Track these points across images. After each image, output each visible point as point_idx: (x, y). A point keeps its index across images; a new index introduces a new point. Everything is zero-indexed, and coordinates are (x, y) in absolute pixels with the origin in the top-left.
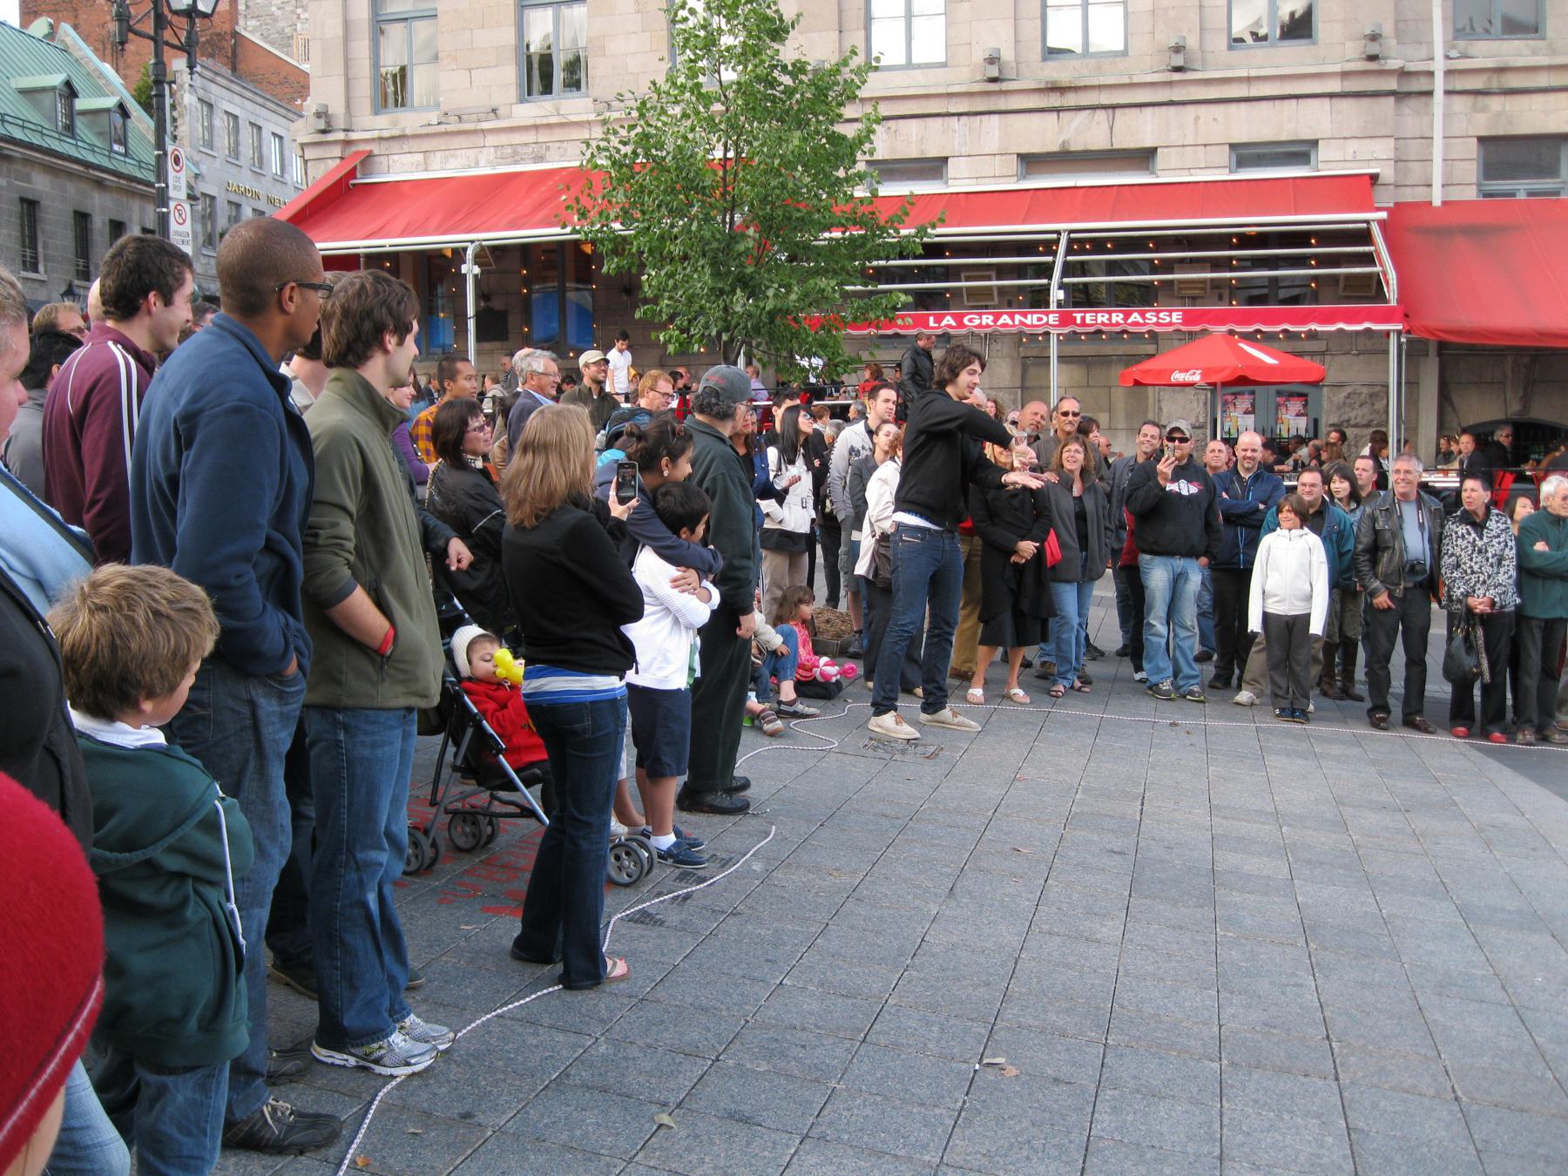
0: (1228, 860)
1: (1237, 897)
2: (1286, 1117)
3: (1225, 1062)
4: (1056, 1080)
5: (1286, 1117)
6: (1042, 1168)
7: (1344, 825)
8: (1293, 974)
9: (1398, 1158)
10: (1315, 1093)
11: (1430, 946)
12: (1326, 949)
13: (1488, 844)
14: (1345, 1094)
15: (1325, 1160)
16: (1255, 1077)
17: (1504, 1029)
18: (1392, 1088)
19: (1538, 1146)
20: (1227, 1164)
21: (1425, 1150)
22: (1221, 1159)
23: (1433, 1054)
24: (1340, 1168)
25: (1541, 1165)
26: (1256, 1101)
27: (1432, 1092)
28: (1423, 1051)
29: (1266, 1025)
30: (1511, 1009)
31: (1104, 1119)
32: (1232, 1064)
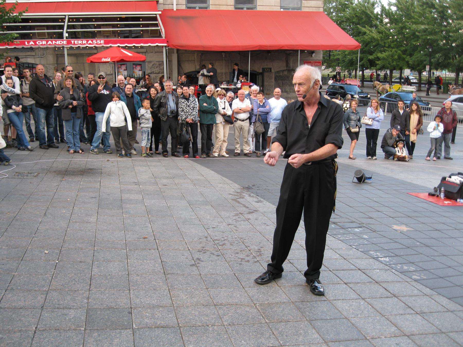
0: (126, 196)
1: (128, 206)
2: (145, 261)
3: (128, 250)
4: (81, 262)
5: (145, 261)
6: (79, 286)
7: (157, 184)
8: (145, 224)
11: (181, 212)
12: (153, 216)
13: (195, 185)
15: (156, 270)
16: (136, 252)
17: (200, 231)
18: (172, 250)
20: (130, 276)
22: (128, 275)
23: (182, 239)
26: (137, 258)
27: (183, 249)
28: (180, 239)
29: (138, 238)
31: (95, 270)
32: (130, 250)
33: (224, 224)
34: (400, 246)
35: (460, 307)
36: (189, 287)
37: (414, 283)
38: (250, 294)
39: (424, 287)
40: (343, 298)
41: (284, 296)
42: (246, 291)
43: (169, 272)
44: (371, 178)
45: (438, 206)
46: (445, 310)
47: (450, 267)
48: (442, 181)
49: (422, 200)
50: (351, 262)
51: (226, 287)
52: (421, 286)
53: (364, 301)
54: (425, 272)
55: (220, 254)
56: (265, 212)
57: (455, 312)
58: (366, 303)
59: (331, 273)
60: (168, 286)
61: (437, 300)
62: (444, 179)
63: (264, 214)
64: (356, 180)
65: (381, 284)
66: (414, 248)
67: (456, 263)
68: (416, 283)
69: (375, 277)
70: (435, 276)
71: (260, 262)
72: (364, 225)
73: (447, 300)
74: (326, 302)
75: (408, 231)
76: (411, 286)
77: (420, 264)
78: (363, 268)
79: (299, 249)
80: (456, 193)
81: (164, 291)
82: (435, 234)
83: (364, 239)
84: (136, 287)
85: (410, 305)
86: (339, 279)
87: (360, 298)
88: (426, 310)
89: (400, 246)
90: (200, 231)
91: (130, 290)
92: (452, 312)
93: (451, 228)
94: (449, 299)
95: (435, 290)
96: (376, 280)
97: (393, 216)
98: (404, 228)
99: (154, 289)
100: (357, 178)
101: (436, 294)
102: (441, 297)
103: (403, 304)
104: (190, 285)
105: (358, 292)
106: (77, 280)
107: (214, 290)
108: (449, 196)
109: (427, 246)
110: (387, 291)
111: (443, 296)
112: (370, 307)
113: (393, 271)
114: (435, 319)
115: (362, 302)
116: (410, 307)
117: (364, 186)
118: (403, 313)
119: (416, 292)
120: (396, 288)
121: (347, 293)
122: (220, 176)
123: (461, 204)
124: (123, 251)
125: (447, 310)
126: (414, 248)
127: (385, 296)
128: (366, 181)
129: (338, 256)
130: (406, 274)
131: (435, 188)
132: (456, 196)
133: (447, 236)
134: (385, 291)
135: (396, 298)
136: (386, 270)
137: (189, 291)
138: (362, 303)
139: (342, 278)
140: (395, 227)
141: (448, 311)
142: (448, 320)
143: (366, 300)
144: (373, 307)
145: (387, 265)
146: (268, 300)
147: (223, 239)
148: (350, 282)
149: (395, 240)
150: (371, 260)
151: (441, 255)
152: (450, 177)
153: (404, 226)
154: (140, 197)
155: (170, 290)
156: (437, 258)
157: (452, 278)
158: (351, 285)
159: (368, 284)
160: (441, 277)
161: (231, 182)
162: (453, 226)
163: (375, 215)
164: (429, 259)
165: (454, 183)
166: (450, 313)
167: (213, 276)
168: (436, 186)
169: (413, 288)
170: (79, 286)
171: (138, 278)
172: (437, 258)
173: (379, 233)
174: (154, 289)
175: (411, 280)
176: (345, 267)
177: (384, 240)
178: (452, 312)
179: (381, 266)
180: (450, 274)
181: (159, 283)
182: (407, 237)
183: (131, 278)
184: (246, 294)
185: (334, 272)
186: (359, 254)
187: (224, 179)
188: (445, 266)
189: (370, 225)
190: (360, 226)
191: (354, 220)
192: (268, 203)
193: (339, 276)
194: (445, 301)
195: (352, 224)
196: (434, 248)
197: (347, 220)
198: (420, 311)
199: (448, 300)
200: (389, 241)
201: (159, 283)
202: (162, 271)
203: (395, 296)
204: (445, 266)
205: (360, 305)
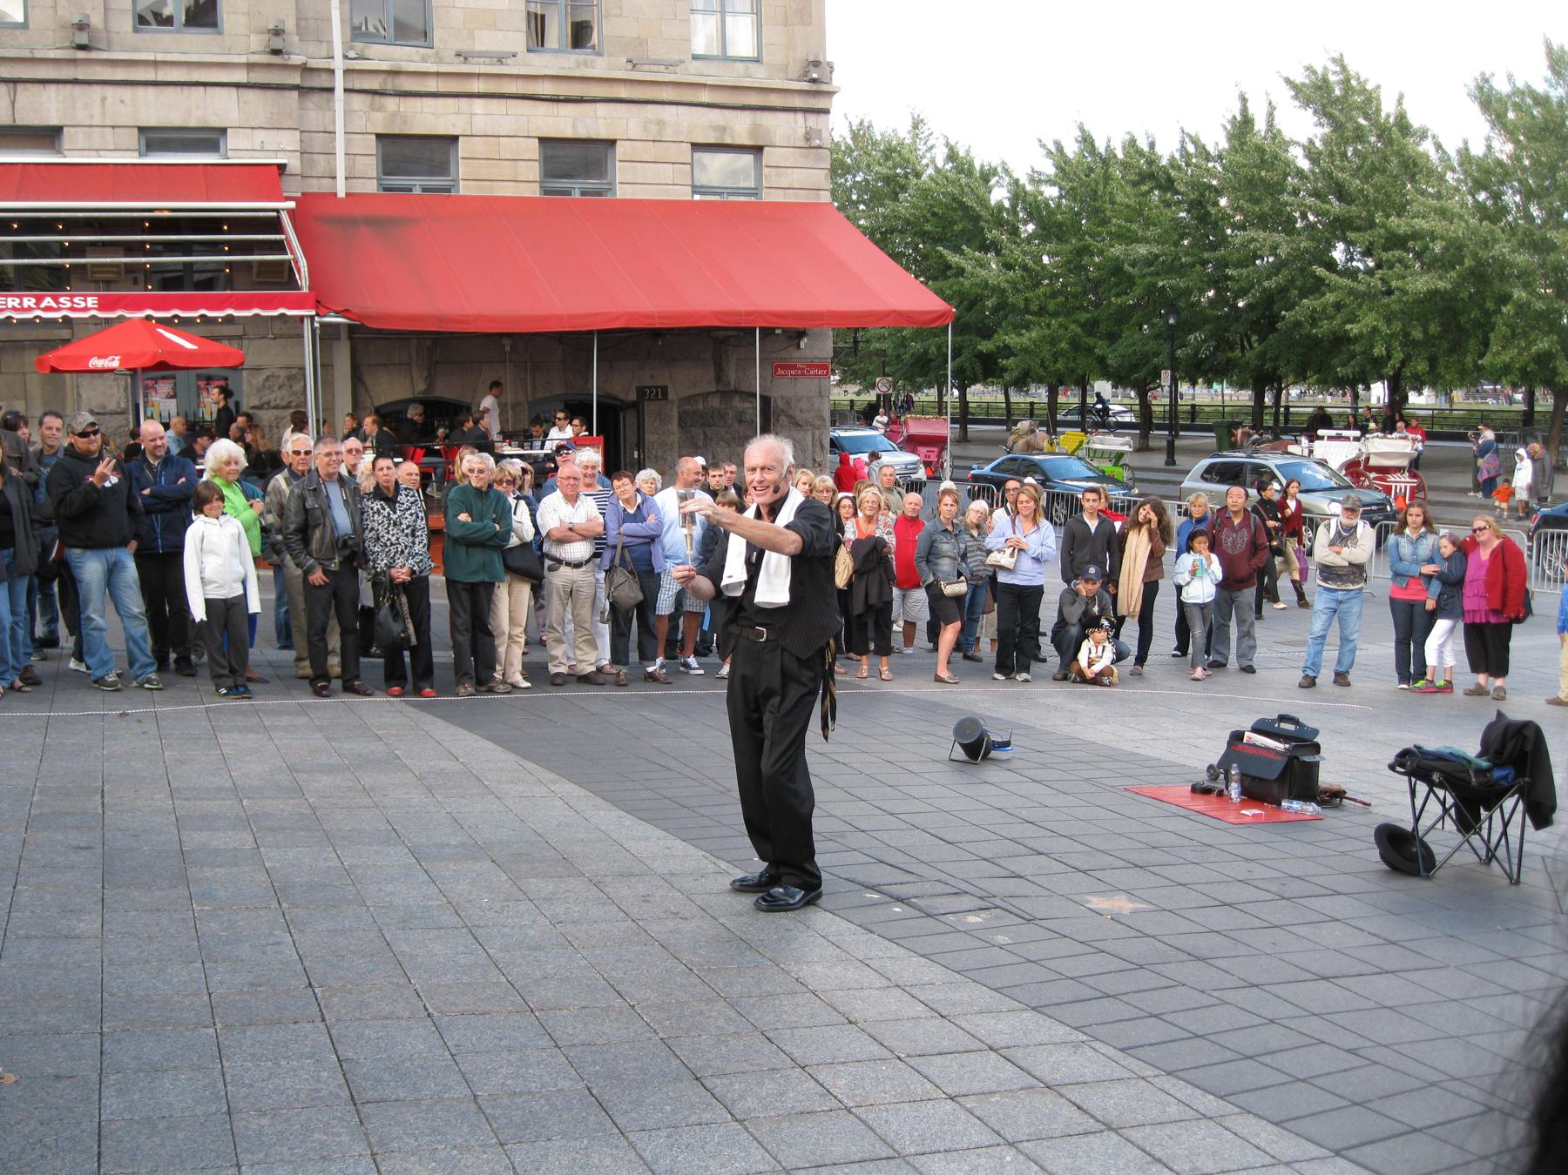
0: (195, 838)
1: (208, 873)
2: (283, 1063)
3: (219, 1026)
4: (57, 1077)
5: (283, 1063)
6: (59, 1163)
9: (386, 1076)
10: (306, 1036)
11: (390, 888)
14: (333, 1032)
16: (249, 1033)
17: (461, 949)
18: (373, 1018)
20: (236, 1116)
21: (408, 1064)
23: (403, 981)
24: (338, 1096)
26: (253, 1055)
27: (407, 1014)
29: (252, 985)
31: (112, 1103)
32: (227, 1026)
33: (541, 920)
34: (1116, 964)
35: (1311, 1147)
36: (440, 1142)
37: (1167, 1083)
38: (647, 1155)
39: (1198, 1091)
40: (949, 1145)
41: (757, 1153)
42: (632, 1145)
43: (369, 1095)
44: (1007, 744)
45: (1224, 825)
46: (1268, 1160)
47: (1272, 1021)
48: (1229, 744)
49: (1174, 809)
50: (964, 1024)
51: (564, 1135)
52: (1190, 1090)
54: (1197, 1041)
56: (672, 874)
57: (1297, 1166)
58: (1021, 1158)
59: (901, 1065)
60: (370, 1145)
61: (1238, 1129)
62: (1237, 737)
63: (668, 879)
64: (960, 753)
65: (1063, 1090)
66: (1159, 968)
68: (1174, 1080)
69: (1043, 1071)
70: (1229, 1055)
71: (670, 1042)
72: (997, 901)
73: (1270, 1127)
74: (892, 1162)
75: (1135, 912)
76: (1159, 1093)
77: (1181, 1019)
78: (1003, 1044)
79: (794, 993)
80: (1276, 780)
81: (357, 1163)
82: (1219, 919)
84: (261, 1156)
85: (1159, 1153)
86: (928, 1085)
87: (1001, 1141)
89: (1116, 964)
90: (461, 949)
91: (239, 1166)
92: (1287, 1164)
93: (1268, 896)
94: (1276, 1124)
95: (1232, 1099)
96: (1048, 1079)
97: (1085, 867)
98: (1123, 905)
99: (323, 1158)
100: (964, 746)
101: (1237, 1110)
102: (1254, 1121)
103: (1138, 1152)
104: (445, 1134)
105: (993, 1121)
106: (49, 1141)
107: (525, 1146)
108: (1256, 792)
110: (1085, 1112)
111: (1256, 1115)
113: (1098, 1045)
116: (1159, 1161)
117: (990, 773)
119: (1174, 1110)
120: (1110, 1102)
121: (959, 1127)
122: (512, 757)
123: (1293, 817)
124: (202, 1030)
126: (1159, 968)
127: (1080, 1129)
128: (993, 754)
129: (921, 1007)
130: (1140, 1052)
131: (1211, 767)
132: (1275, 789)
133: (1258, 923)
134: (1077, 1114)
135: (1113, 1135)
136: (1077, 1045)
137: (442, 1155)
138: (1008, 1159)
139: (938, 1081)
140: (1096, 902)
141: (1278, 1162)
143: (1020, 1146)
144: (1042, 1168)
145: (1076, 1029)
146: (707, 1168)
147: (539, 974)
148: (964, 1091)
150: (1027, 1015)
151: (1241, 984)
153: (1123, 896)
154: (245, 840)
155: (378, 1158)
156: (1229, 996)
157: (1279, 1056)
159: (1022, 1094)
160: (1248, 1058)
161: (552, 776)
162: (1274, 889)
163: (1028, 865)
164: (1206, 1001)
166: (1282, 1169)
167: (519, 1101)
168: (1215, 762)
169: (1164, 1096)
170: (59, 1163)
171: (265, 1121)
172: (1229, 996)
173: (1043, 923)
174: (323, 1158)
175: (1157, 1072)
176: (946, 1045)
177: (1064, 947)
178: (1287, 1164)
179: (1062, 1031)
180: (1274, 1045)
181: (339, 1135)
182: (1134, 933)
183: (240, 1125)
184: (632, 1156)
185: (911, 1061)
186: (985, 997)
187: (529, 765)
188: (1258, 1021)
189: (1014, 901)
190: (983, 904)
191: (964, 886)
192: (679, 846)
193: (929, 1072)
195: (957, 899)
196: (1219, 963)
197: (940, 888)
199: (1275, 1129)
200: (1080, 949)
201: (339, 1135)
202: (345, 1094)
203: (1110, 1129)
204: (1258, 1021)
205: (1002, 1166)
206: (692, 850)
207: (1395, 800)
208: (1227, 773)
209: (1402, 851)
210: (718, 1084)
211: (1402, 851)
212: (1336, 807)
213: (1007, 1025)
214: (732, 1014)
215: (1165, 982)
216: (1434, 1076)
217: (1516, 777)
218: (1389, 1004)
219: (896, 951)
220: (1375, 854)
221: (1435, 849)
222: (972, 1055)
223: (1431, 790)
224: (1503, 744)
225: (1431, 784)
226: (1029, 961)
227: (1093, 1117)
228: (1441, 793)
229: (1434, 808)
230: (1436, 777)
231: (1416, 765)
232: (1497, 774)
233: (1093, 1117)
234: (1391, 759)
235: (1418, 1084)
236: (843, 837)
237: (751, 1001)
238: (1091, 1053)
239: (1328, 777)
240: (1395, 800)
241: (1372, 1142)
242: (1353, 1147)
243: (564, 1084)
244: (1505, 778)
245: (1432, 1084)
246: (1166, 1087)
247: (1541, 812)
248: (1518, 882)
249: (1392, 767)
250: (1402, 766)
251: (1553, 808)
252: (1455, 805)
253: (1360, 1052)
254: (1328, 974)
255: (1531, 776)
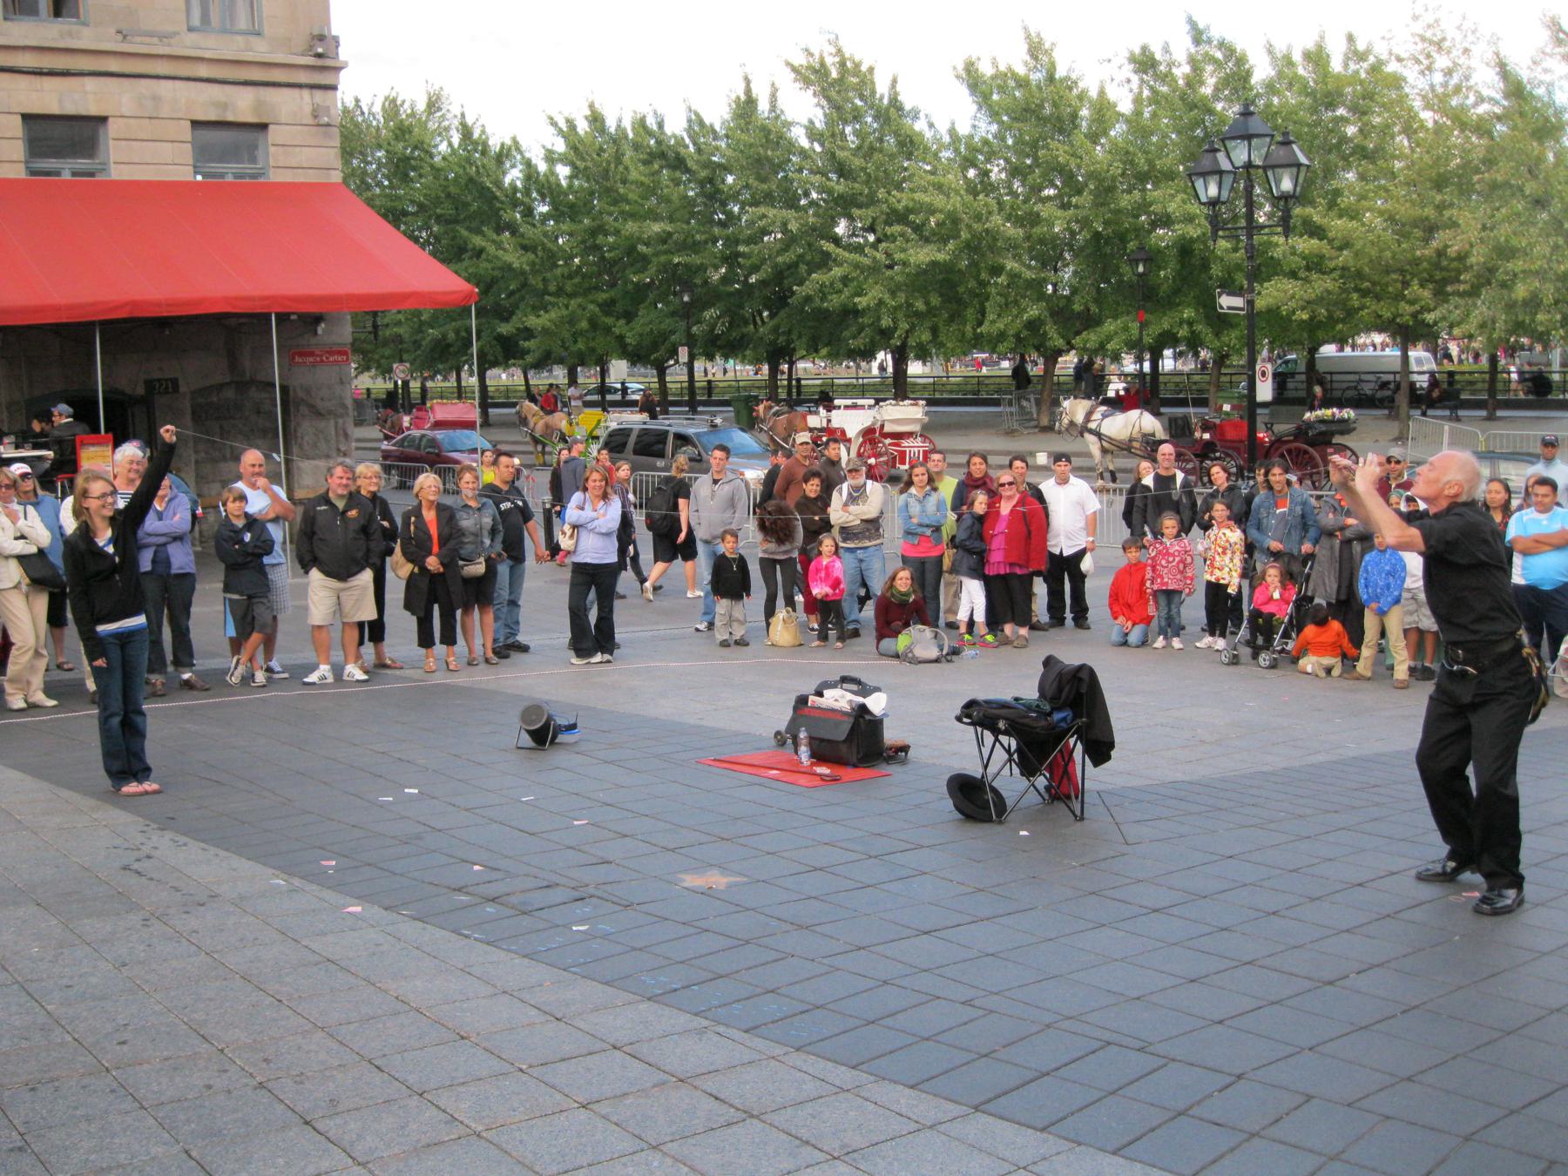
19: (76, 1108)
25: (83, 1125)
30: (16, 987)
35: (951, 1106)
37: (798, 1059)
39: (830, 1064)
44: (573, 727)
46: (913, 1126)
47: (885, 982)
48: (795, 709)
50: (581, 1025)
52: (822, 1063)
53: (658, 1155)
55: (115, 1084)
56: (242, 898)
57: (942, 1128)
58: (669, 1161)
59: (525, 1078)
62: (802, 701)
64: (527, 740)
65: (697, 1082)
67: (900, 966)
68: (804, 1056)
71: (270, 1085)
72: (591, 890)
73: (907, 1091)
75: (730, 886)
83: (606, 936)
85: (804, 1133)
86: (558, 1097)
87: (645, 1146)
88: (857, 1141)
93: (854, 856)
98: (717, 880)
100: (528, 732)
101: (872, 1078)
103: (784, 1136)
108: (824, 752)
109: (801, 927)
111: (891, 1081)
112: (686, 1169)
113: (721, 1029)
114: (891, 1164)
115: (655, 1159)
116: (807, 1143)
118: (791, 1167)
119: (810, 1087)
125: (917, 1126)
127: (722, 1121)
128: (561, 738)
129: (534, 1012)
131: (778, 733)
132: (844, 749)
135: (755, 1121)
136: (702, 1032)
138: (656, 1164)
140: (691, 881)
142: (930, 1156)
144: (691, 1168)
145: (696, 1014)
148: (596, 1096)
149: (699, 924)
150: (643, 1006)
151: (848, 948)
152: (820, 694)
153: (716, 872)
157: (900, 1016)
158: (604, 1108)
165: (833, 710)
166: (928, 1133)
168: (783, 727)
179: (683, 1020)
185: (535, 1072)
187: (66, 794)
188: (872, 983)
189: (608, 888)
190: (577, 894)
192: (244, 866)
194: (903, 1098)
195: (550, 891)
198: (842, 1147)
203: (752, 1116)
206: (259, 868)
207: (966, 751)
208: (795, 739)
209: (972, 798)
210: (330, 1126)
211: (972, 798)
212: (904, 762)
213: (627, 1018)
214: (335, 1046)
215: (774, 955)
216: (1047, 1018)
217: (1075, 717)
218: (991, 951)
219: (497, 955)
220: (950, 803)
221: (1004, 794)
222: (596, 1057)
223: (997, 740)
224: (1060, 689)
225: (996, 732)
226: (634, 949)
227: (732, 1106)
228: (1004, 739)
229: (1000, 756)
230: (1002, 725)
231: (980, 715)
232: (1057, 716)
233: (732, 1106)
234: (958, 712)
235: (1035, 1028)
236: (420, 838)
237: (352, 1027)
238: (716, 1038)
239: (891, 735)
240: (966, 751)
241: (1005, 1093)
242: (990, 1101)
243: (158, 1150)
244: (1064, 719)
245: (1048, 1026)
246: (799, 1063)
247: (1100, 750)
248: (1082, 819)
249: (959, 719)
250: (968, 716)
251: (1111, 745)
252: (1019, 750)
253: (976, 1002)
254: (928, 928)
255: (1088, 716)
